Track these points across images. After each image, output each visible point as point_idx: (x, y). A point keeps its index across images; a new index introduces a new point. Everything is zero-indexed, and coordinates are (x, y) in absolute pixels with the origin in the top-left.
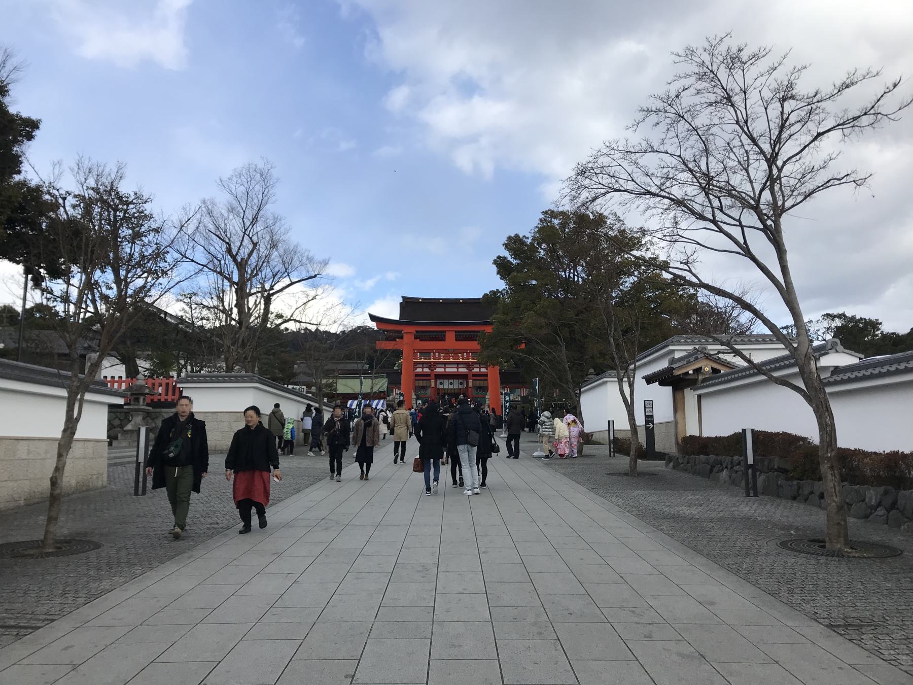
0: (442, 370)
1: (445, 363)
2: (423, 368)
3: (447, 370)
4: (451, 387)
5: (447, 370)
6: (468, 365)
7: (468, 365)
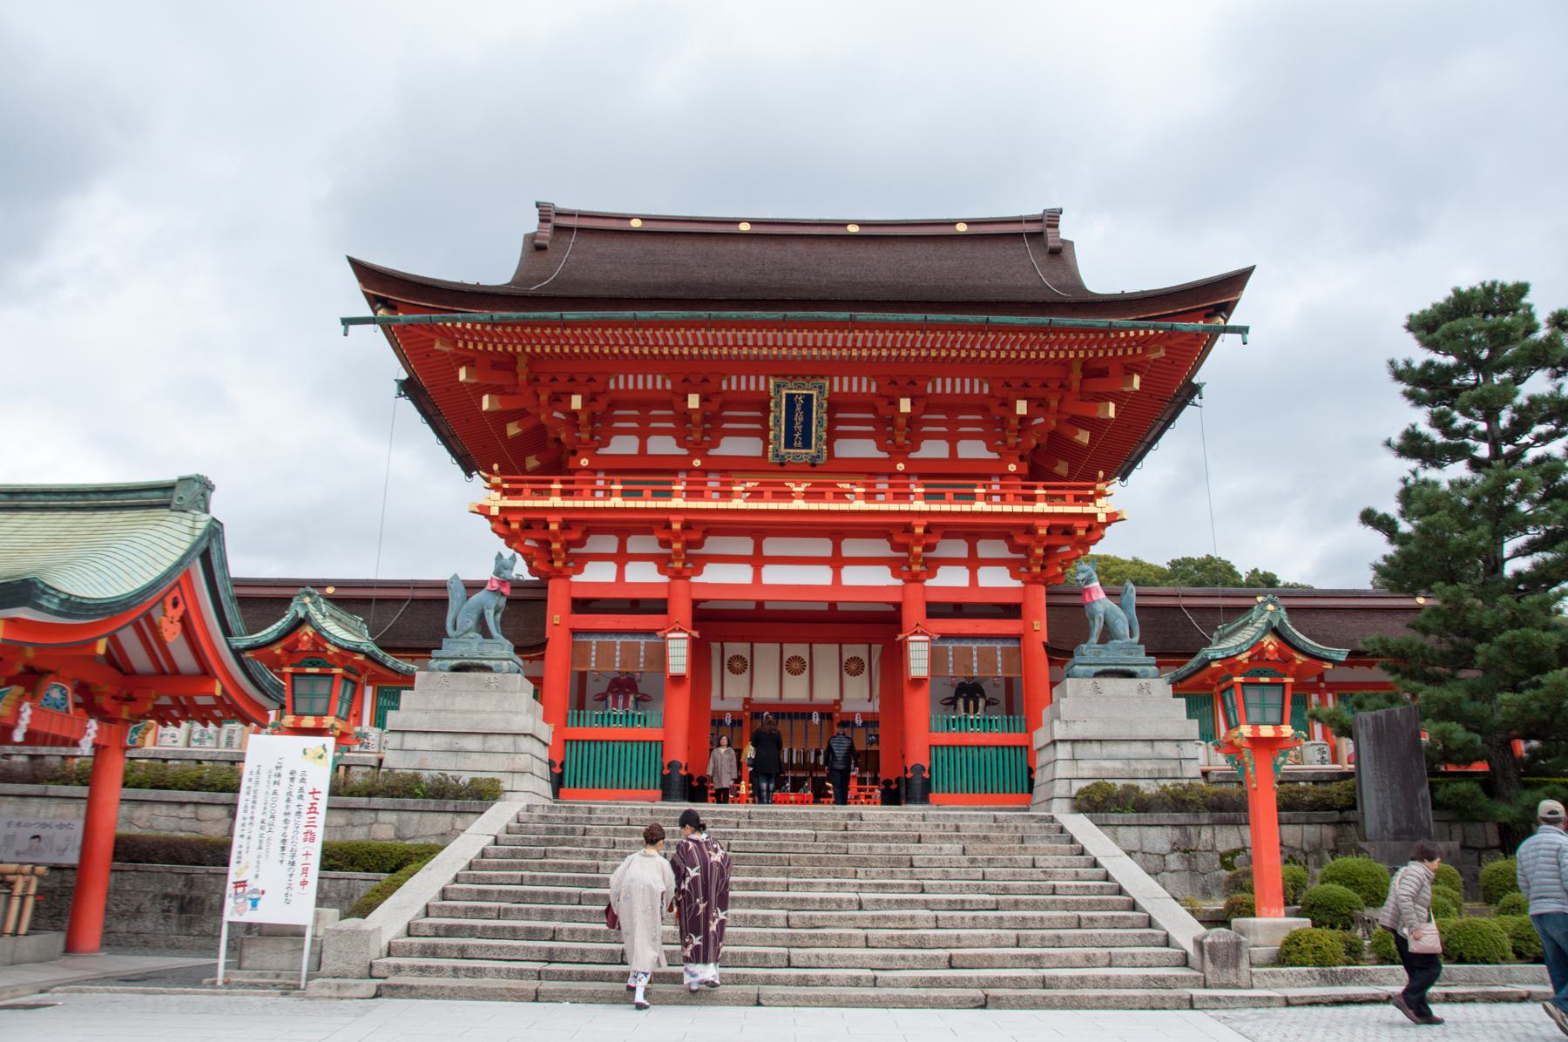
0: (741, 575)
1: (758, 528)
2: (622, 558)
3: (774, 575)
4: (796, 691)
5: (774, 575)
6: (909, 545)
7: (909, 545)
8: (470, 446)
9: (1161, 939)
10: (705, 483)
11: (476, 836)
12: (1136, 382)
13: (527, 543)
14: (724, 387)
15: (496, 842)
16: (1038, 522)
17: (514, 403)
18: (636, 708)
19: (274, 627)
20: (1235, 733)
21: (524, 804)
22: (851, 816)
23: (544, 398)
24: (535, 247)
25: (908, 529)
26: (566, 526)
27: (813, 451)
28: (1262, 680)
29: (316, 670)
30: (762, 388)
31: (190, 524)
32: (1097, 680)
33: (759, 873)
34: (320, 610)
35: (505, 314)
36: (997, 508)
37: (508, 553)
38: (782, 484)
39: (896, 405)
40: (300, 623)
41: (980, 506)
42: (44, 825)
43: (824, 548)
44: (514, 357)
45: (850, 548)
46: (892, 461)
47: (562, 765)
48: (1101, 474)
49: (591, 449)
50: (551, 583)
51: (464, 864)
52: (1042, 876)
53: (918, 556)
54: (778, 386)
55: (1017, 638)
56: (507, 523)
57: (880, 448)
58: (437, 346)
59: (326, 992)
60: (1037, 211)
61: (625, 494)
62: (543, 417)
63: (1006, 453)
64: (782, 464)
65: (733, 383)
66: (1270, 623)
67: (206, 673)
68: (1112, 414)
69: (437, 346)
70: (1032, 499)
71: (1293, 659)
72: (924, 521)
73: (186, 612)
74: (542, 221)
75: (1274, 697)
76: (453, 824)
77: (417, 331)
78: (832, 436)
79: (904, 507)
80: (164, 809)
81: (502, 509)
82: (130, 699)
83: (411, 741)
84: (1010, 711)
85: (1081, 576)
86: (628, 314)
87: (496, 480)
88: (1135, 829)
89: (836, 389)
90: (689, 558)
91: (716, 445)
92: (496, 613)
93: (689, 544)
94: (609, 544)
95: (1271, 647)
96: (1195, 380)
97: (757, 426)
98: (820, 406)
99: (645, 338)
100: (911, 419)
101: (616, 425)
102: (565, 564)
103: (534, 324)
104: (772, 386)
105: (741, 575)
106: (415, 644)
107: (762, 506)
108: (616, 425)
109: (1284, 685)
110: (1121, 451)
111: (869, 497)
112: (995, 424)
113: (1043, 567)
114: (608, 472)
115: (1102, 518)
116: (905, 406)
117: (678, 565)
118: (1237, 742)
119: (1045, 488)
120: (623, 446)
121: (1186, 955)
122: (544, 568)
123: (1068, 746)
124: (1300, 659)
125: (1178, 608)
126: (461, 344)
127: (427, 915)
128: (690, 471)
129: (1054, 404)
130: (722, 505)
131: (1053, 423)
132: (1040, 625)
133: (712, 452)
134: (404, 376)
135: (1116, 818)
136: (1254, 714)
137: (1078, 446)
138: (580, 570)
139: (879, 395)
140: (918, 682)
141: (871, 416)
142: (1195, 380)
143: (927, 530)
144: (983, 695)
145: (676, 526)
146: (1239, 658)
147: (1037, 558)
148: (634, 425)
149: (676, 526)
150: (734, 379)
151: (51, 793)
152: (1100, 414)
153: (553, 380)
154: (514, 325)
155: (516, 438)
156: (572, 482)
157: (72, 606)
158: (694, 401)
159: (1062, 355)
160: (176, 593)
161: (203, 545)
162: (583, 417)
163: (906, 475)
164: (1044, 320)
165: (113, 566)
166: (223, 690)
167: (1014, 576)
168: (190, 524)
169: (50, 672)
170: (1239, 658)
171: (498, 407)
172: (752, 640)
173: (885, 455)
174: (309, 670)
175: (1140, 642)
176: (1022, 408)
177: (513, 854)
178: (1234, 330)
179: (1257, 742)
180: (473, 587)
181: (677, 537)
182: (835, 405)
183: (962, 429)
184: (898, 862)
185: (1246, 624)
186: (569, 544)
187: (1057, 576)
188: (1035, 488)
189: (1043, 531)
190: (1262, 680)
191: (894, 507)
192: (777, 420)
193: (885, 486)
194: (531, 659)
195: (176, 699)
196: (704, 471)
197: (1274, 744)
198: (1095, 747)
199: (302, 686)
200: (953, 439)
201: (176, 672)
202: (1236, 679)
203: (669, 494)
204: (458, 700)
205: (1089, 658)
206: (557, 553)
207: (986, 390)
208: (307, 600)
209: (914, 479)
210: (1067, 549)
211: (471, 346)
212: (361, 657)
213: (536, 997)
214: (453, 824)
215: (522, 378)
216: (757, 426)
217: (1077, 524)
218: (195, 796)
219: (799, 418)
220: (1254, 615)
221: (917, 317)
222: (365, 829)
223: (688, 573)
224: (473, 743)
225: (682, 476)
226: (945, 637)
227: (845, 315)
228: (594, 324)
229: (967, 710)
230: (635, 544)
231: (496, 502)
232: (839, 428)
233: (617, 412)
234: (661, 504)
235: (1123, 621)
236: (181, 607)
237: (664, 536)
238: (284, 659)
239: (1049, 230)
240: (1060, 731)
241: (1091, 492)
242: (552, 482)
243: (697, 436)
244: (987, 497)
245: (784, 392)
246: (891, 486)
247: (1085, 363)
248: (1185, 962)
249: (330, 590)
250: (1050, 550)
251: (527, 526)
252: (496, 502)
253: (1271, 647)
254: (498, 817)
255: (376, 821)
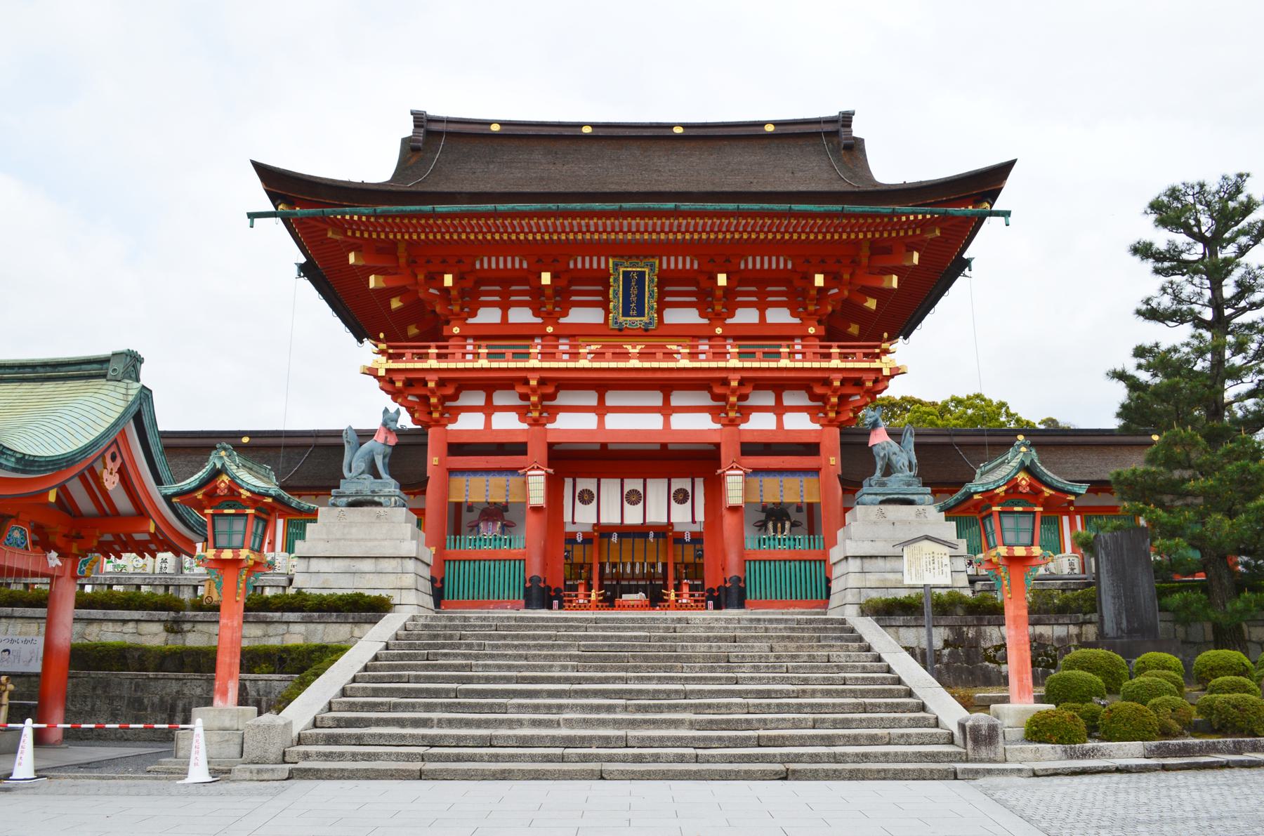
0: (587, 422)
1: (601, 384)
2: (489, 409)
3: (614, 422)
4: (633, 516)
5: (614, 422)
8: (361, 316)
9: (932, 721)
10: (557, 347)
11: (370, 641)
12: (916, 256)
13: (410, 398)
14: (572, 266)
15: (387, 648)
16: (833, 376)
17: (396, 282)
18: (503, 532)
19: (196, 476)
20: (993, 553)
21: (410, 615)
22: (679, 620)
23: (421, 277)
24: (409, 148)
25: (725, 382)
26: (442, 383)
27: (645, 319)
28: (1016, 509)
29: (232, 511)
30: (603, 266)
31: (124, 391)
32: (882, 507)
33: (603, 669)
34: (234, 462)
35: (386, 208)
36: (799, 365)
37: (394, 407)
38: (621, 347)
39: (715, 279)
40: (216, 473)
41: (784, 363)
42: (12, 641)
43: (656, 399)
44: (394, 243)
45: (677, 399)
46: (712, 326)
47: (442, 581)
48: (886, 335)
49: (461, 318)
50: (430, 431)
51: (361, 666)
52: (835, 670)
53: (733, 406)
54: (616, 265)
55: (816, 471)
56: (392, 382)
57: (702, 316)
58: (330, 234)
59: (248, 776)
60: (833, 112)
61: (489, 356)
62: (421, 294)
63: (806, 317)
64: (620, 330)
65: (581, 263)
66: (1022, 462)
67: (141, 513)
68: (895, 284)
69: (330, 234)
70: (828, 356)
71: (1042, 492)
72: (738, 376)
73: (123, 464)
74: (415, 126)
75: (1026, 523)
76: (352, 632)
77: (313, 223)
78: (662, 306)
79: (722, 364)
80: (110, 627)
81: (388, 370)
82: (79, 537)
83: (315, 565)
84: (811, 531)
85: (868, 420)
86: (490, 207)
87: (383, 346)
88: (913, 630)
89: (665, 266)
90: (546, 409)
91: (566, 314)
92: (384, 457)
93: (545, 397)
94: (478, 399)
95: (1024, 483)
96: (966, 256)
97: (600, 298)
98: (651, 281)
99: (504, 226)
100: (728, 292)
101: (483, 298)
102: (442, 415)
103: (411, 216)
104: (611, 265)
105: (587, 422)
106: (317, 483)
107: (604, 365)
108: (483, 298)
109: (1034, 513)
110: (905, 314)
111: (693, 356)
112: (798, 297)
113: (838, 413)
114: (476, 338)
115: (886, 372)
116: (722, 280)
117: (536, 414)
118: (995, 560)
119: (839, 347)
120: (488, 316)
121: (952, 734)
122: (425, 418)
123: (858, 561)
124: (1048, 492)
125: (950, 445)
126: (349, 233)
127: (330, 710)
128: (544, 336)
129: (846, 277)
130: (571, 365)
131: (846, 293)
132: (833, 461)
133: (562, 320)
134: (303, 260)
135: (900, 620)
136: (1009, 537)
137: (868, 310)
138: (454, 420)
139: (700, 271)
140: (735, 509)
141: (694, 289)
142: (966, 256)
143: (742, 382)
144: (789, 519)
145: (533, 383)
146: (997, 491)
147: (833, 406)
148: (497, 298)
149: (533, 383)
150: (579, 259)
151: (16, 614)
152: (885, 285)
153: (428, 262)
154: (394, 217)
155: (399, 310)
156: (447, 347)
157: (26, 463)
158: (546, 278)
159: (853, 236)
160: (113, 449)
161: (135, 409)
162: (454, 293)
163: (724, 337)
164: (837, 208)
165: (62, 426)
166: (157, 527)
167: (813, 420)
168: (124, 391)
169: (10, 517)
170: (997, 491)
171: (382, 285)
172: (599, 475)
173: (705, 321)
174: (226, 511)
175: (918, 475)
176: (819, 280)
177: (401, 657)
178: (998, 214)
179: (1012, 560)
180: (365, 435)
181: (534, 390)
182: (665, 279)
183: (770, 299)
184: (717, 659)
185: (1003, 463)
186: (444, 399)
187: (850, 420)
188: (830, 347)
189: (837, 383)
190: (1016, 509)
191: (713, 365)
192: (616, 293)
193: (706, 347)
194: (415, 494)
195: (117, 536)
196: (557, 336)
197: (1025, 561)
198: (880, 562)
199: (221, 525)
200: (762, 307)
201: (116, 512)
202: (994, 509)
203: (527, 356)
204: (354, 530)
205: (876, 489)
206: (435, 406)
207: (790, 266)
208: (223, 453)
209: (730, 341)
210: (858, 397)
211: (358, 235)
212: (270, 500)
213: (421, 775)
214: (352, 632)
215: (402, 261)
216: (600, 298)
217: (864, 376)
218: (136, 615)
219: (634, 291)
220: (1009, 456)
221: (731, 206)
222: (279, 639)
223: (544, 421)
224: (367, 565)
225: (538, 341)
226: (757, 471)
227: (671, 205)
228: (461, 215)
229: (775, 531)
230: (500, 399)
231: (383, 364)
232: (668, 299)
233: (483, 288)
234: (520, 365)
235: (904, 456)
236: (119, 461)
237: (524, 390)
238: (205, 503)
239: (843, 129)
240: (851, 548)
241: (877, 351)
242: (429, 347)
243: (549, 307)
244: (791, 355)
245: (621, 270)
246: (711, 347)
247: (873, 241)
248: (951, 741)
249: (245, 440)
250: (844, 399)
251: (409, 383)
252: (383, 364)
253: (1024, 483)
254: (389, 626)
255: (288, 632)
